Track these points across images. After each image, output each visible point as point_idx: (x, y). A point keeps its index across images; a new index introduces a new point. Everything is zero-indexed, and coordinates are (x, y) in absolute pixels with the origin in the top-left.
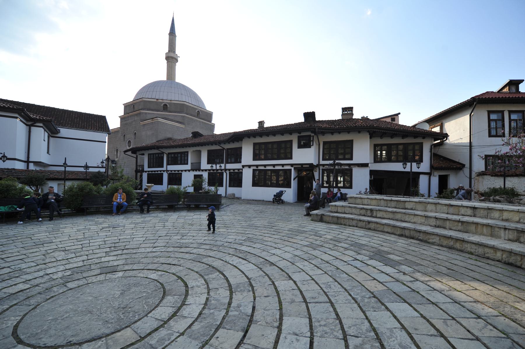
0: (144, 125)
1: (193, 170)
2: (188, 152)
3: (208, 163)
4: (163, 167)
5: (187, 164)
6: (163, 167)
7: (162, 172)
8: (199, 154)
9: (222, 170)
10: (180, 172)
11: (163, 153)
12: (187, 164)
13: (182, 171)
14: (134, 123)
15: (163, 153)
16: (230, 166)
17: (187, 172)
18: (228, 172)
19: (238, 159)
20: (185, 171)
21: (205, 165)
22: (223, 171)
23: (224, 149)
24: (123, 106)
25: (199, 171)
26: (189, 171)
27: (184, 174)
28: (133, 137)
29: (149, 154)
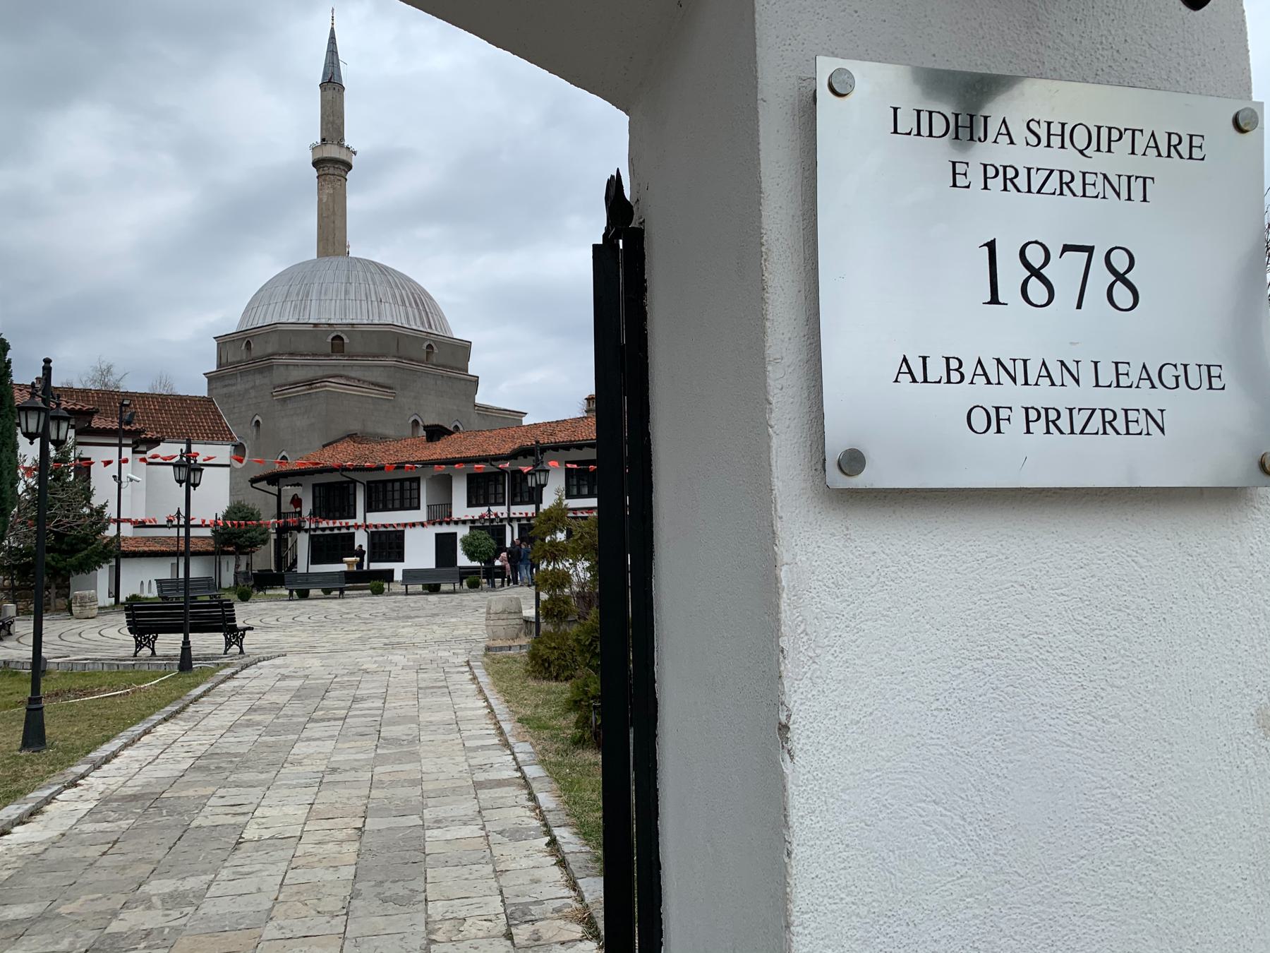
0: (285, 400)
1: (432, 522)
2: (418, 480)
3: (470, 505)
4: (354, 517)
5: (418, 508)
6: (354, 517)
7: (352, 530)
8: (445, 484)
9: (502, 520)
10: (400, 528)
11: (354, 482)
12: (418, 508)
13: (405, 525)
14: (253, 393)
15: (354, 482)
16: (518, 510)
17: (419, 529)
18: (516, 525)
19: (535, 496)
20: (413, 525)
21: (460, 508)
22: (505, 523)
23: (503, 472)
24: (215, 343)
25: (448, 523)
26: (422, 524)
27: (409, 533)
28: (252, 432)
29: (314, 486)
